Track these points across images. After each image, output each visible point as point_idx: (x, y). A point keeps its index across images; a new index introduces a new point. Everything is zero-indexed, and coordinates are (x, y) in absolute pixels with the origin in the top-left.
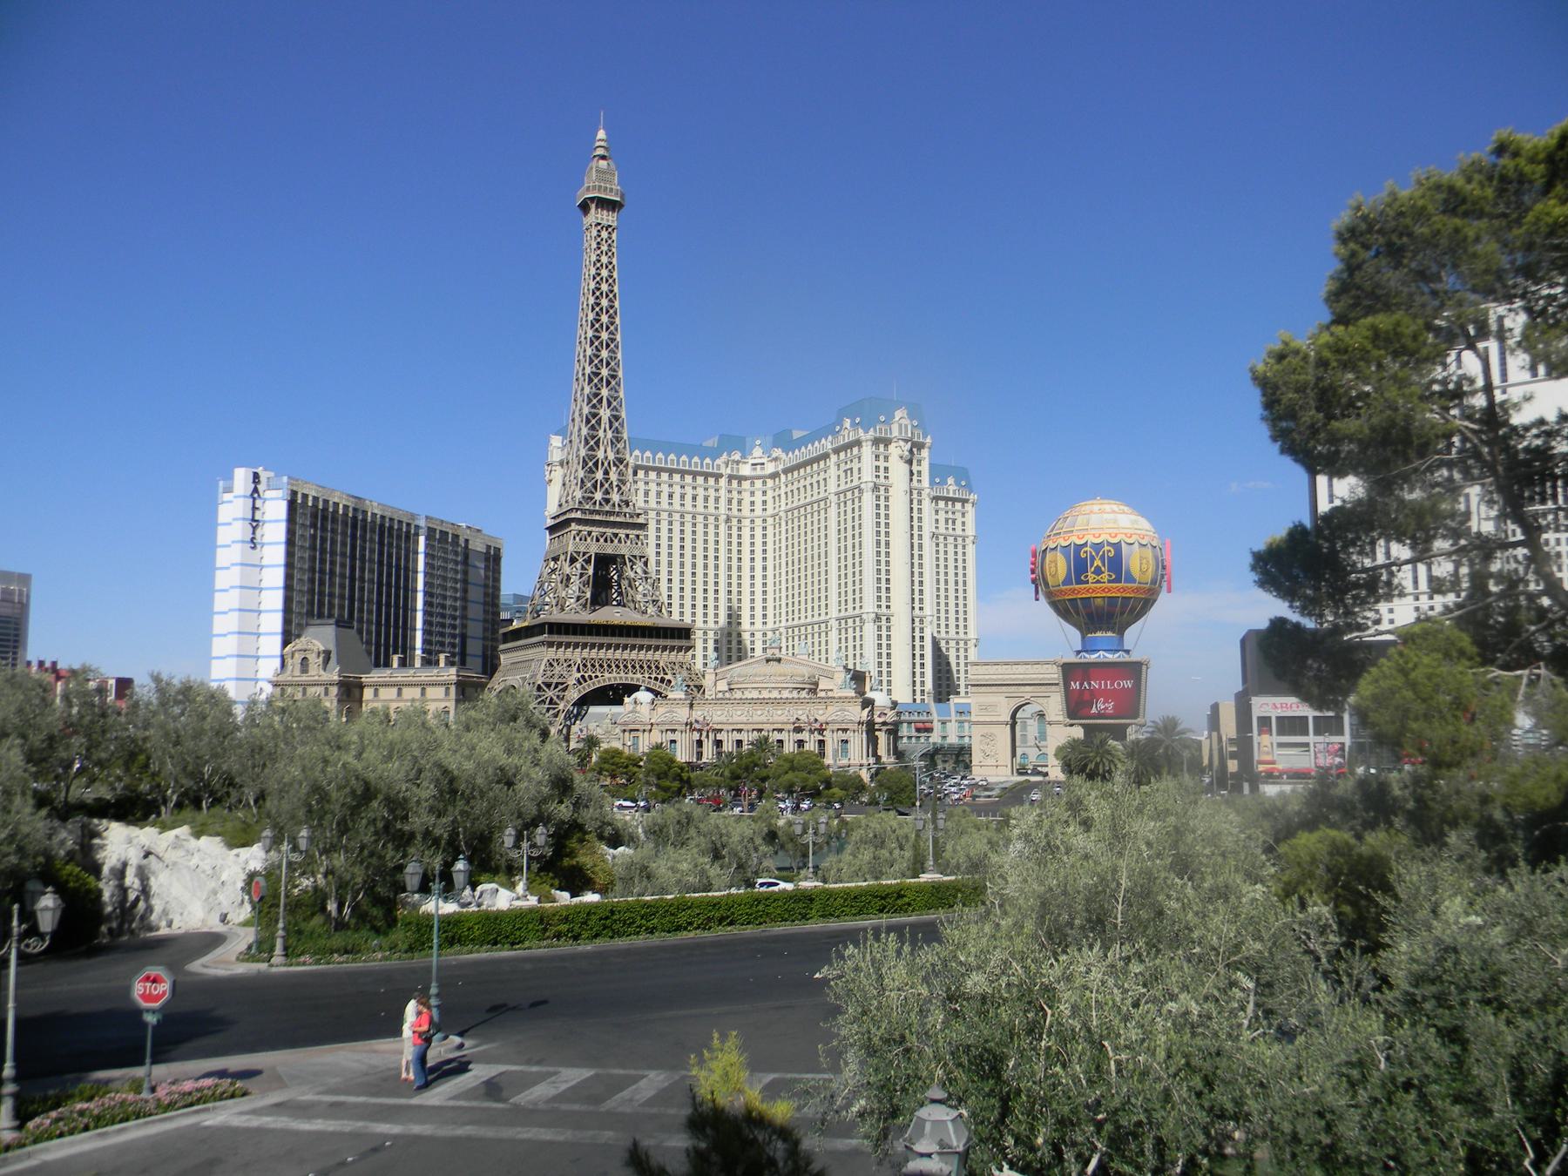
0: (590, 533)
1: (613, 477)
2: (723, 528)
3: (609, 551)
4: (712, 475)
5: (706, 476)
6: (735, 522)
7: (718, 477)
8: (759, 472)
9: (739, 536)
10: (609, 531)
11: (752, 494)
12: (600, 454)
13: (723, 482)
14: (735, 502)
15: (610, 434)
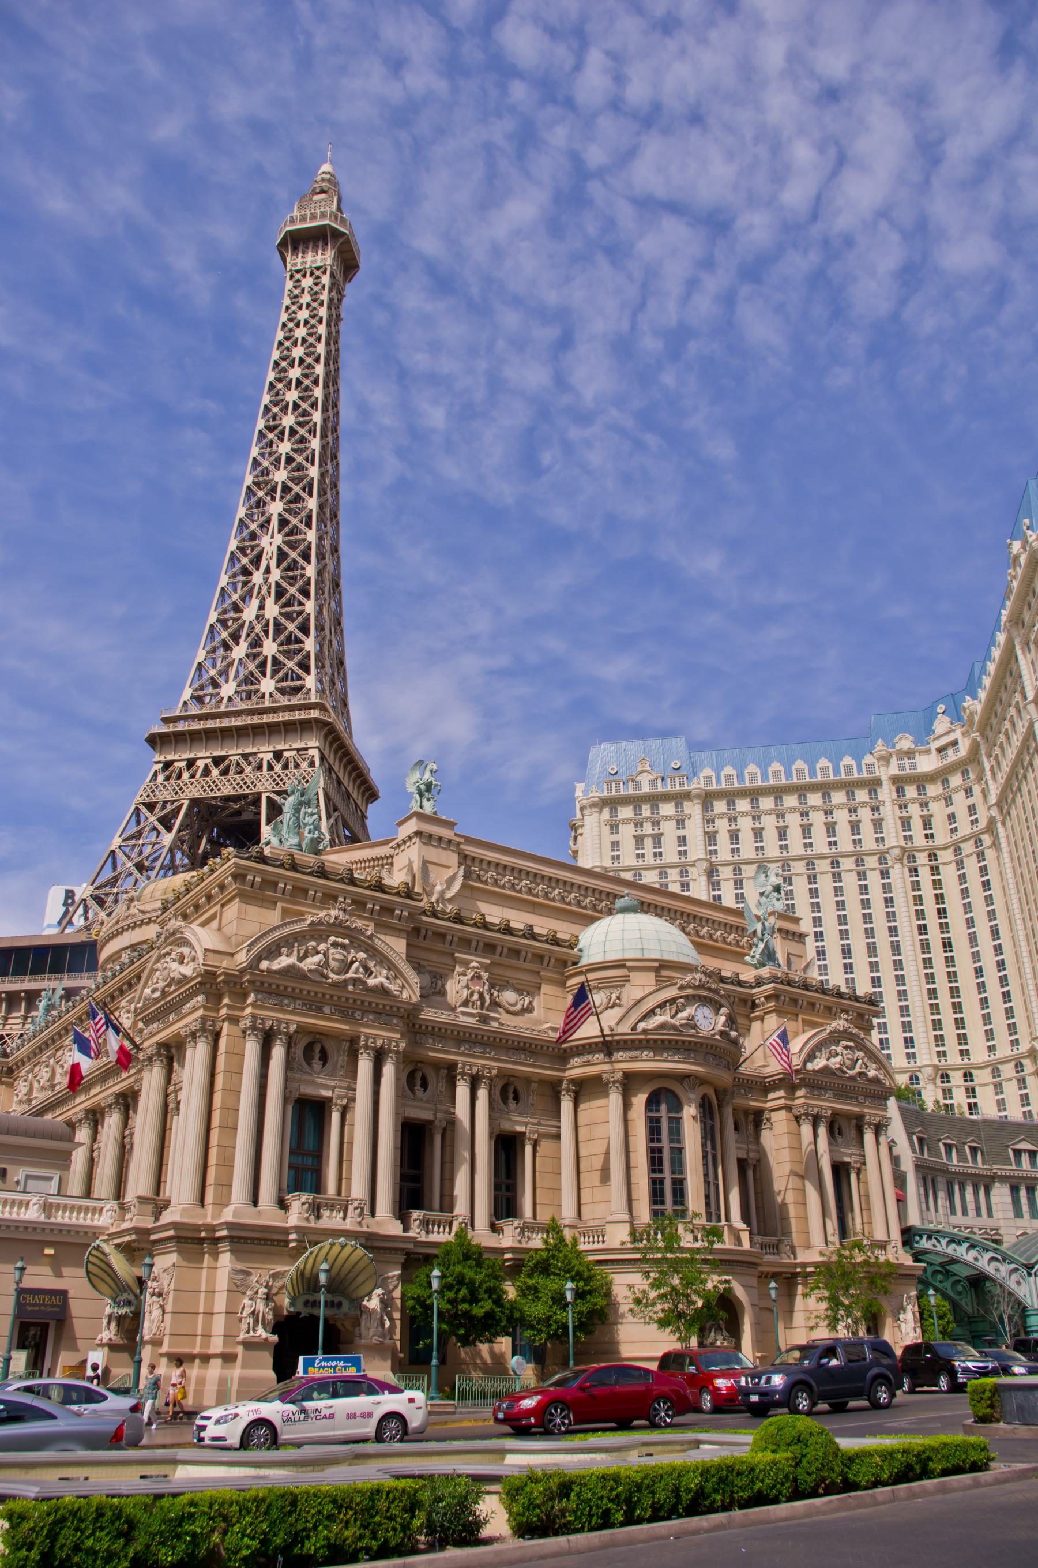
0: (191, 763)
1: (270, 648)
2: (898, 874)
3: (227, 791)
4: (861, 784)
5: (849, 787)
6: (922, 858)
7: (873, 785)
8: (951, 756)
9: (937, 884)
10: (234, 751)
11: (948, 800)
12: (249, 613)
13: (886, 793)
14: (917, 824)
15: (276, 575)
